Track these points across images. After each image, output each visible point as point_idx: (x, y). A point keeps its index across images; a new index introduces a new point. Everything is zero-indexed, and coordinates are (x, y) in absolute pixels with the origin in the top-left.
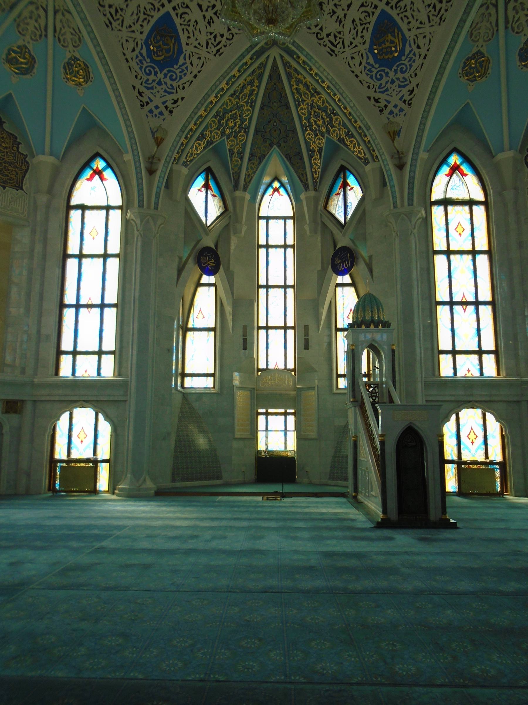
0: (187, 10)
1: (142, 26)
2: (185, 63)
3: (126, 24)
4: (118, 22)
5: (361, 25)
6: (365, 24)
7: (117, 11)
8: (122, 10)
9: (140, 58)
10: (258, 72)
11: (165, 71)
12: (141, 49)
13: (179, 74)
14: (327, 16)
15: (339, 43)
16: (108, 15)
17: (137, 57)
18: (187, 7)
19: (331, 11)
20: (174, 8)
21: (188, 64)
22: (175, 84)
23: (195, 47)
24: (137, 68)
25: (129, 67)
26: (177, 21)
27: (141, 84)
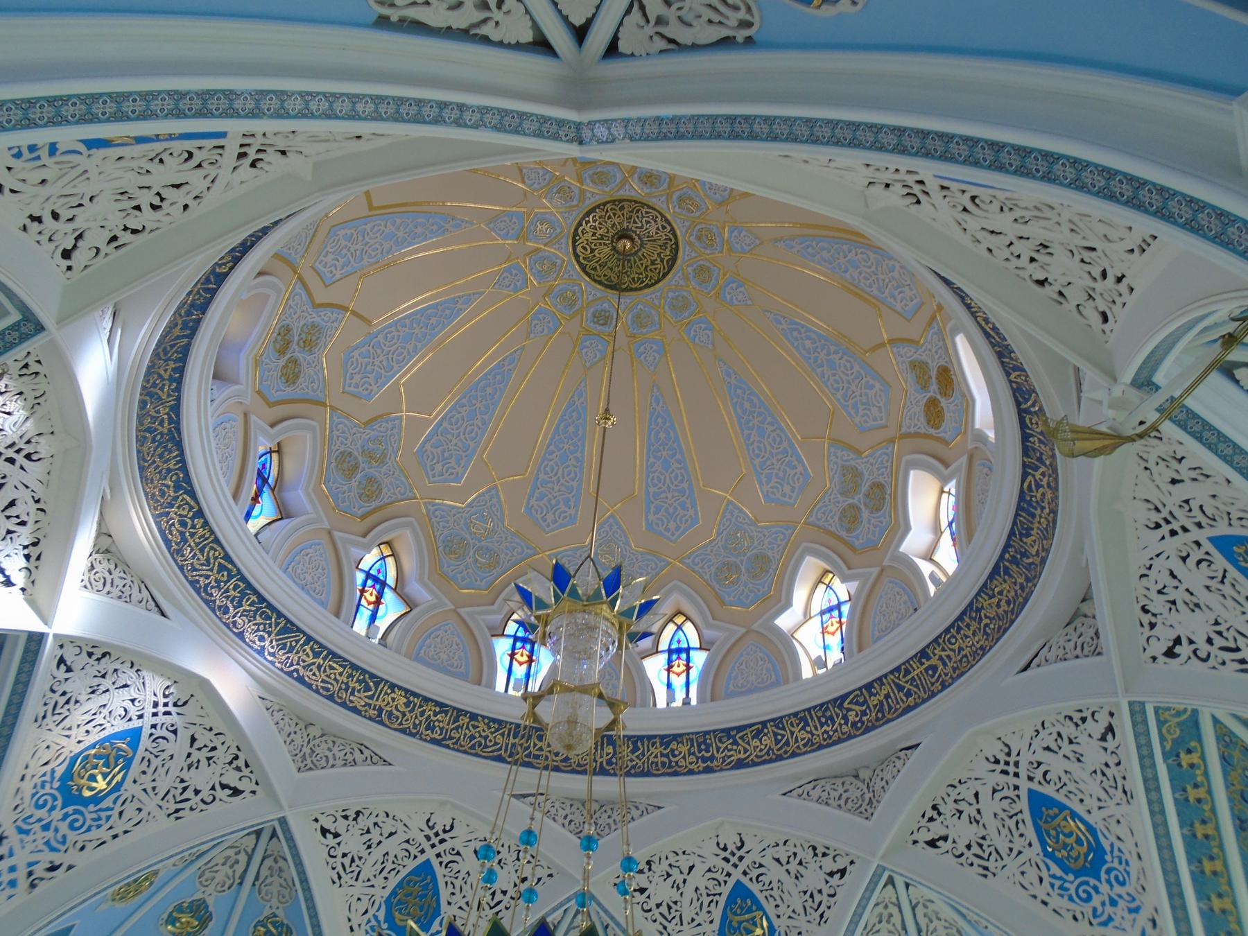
0: (1043, 768)
1: (1021, 835)
2: (1112, 845)
3: (1004, 852)
4: (992, 858)
5: (1222, 582)
6: (1224, 576)
7: (981, 846)
8: (984, 838)
9: (1058, 883)
10: (1236, 754)
11: (1103, 876)
12: (1049, 870)
13: (1121, 868)
14: (1173, 618)
15: (1235, 640)
16: (977, 861)
17: (1052, 885)
18: (1039, 764)
19: (1169, 605)
20: (1030, 779)
21: (1117, 844)
22: (1130, 888)
23: (1100, 808)
24: (1065, 903)
25: (1055, 911)
26: (1048, 790)
27: (1091, 924)
